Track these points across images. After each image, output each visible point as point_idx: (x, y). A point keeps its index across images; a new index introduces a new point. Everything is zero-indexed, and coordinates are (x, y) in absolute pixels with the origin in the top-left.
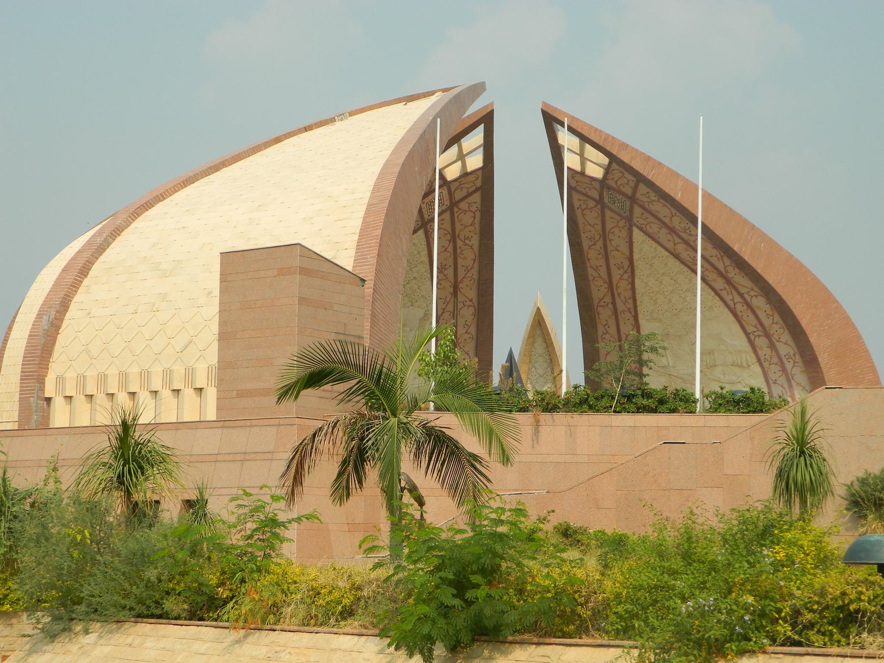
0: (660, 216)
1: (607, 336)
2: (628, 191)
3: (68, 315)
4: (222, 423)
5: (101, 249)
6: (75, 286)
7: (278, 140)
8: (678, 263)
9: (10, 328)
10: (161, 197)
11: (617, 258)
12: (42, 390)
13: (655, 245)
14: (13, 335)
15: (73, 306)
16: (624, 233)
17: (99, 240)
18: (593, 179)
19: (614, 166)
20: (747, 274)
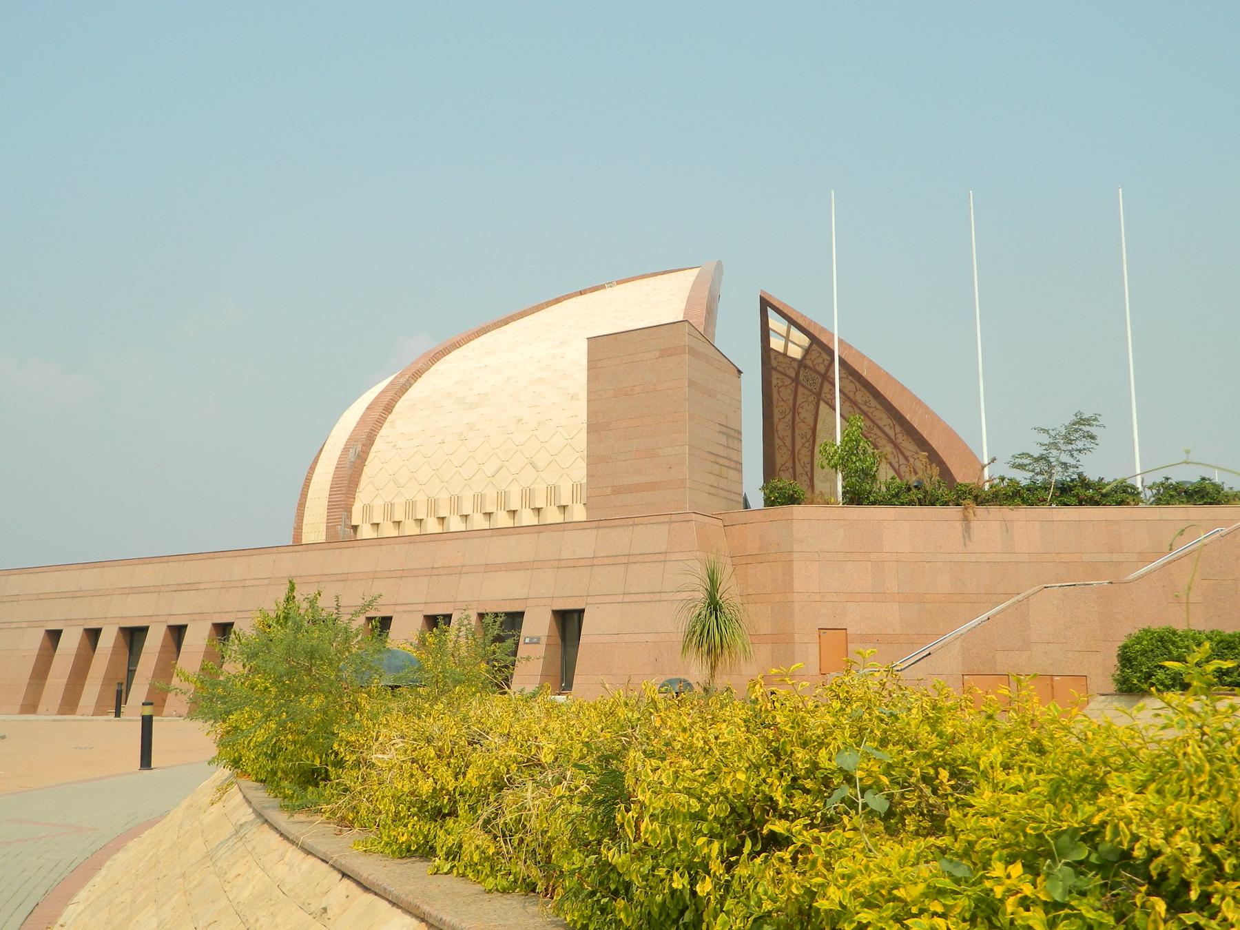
3: (373, 449)
4: (594, 523)
5: (404, 389)
6: (380, 422)
7: (558, 301)
9: (312, 469)
10: (457, 345)
11: (803, 428)
12: (349, 518)
14: (318, 470)
15: (378, 441)
16: (812, 407)
17: (402, 380)
18: (794, 359)
19: (815, 346)
20: (914, 440)
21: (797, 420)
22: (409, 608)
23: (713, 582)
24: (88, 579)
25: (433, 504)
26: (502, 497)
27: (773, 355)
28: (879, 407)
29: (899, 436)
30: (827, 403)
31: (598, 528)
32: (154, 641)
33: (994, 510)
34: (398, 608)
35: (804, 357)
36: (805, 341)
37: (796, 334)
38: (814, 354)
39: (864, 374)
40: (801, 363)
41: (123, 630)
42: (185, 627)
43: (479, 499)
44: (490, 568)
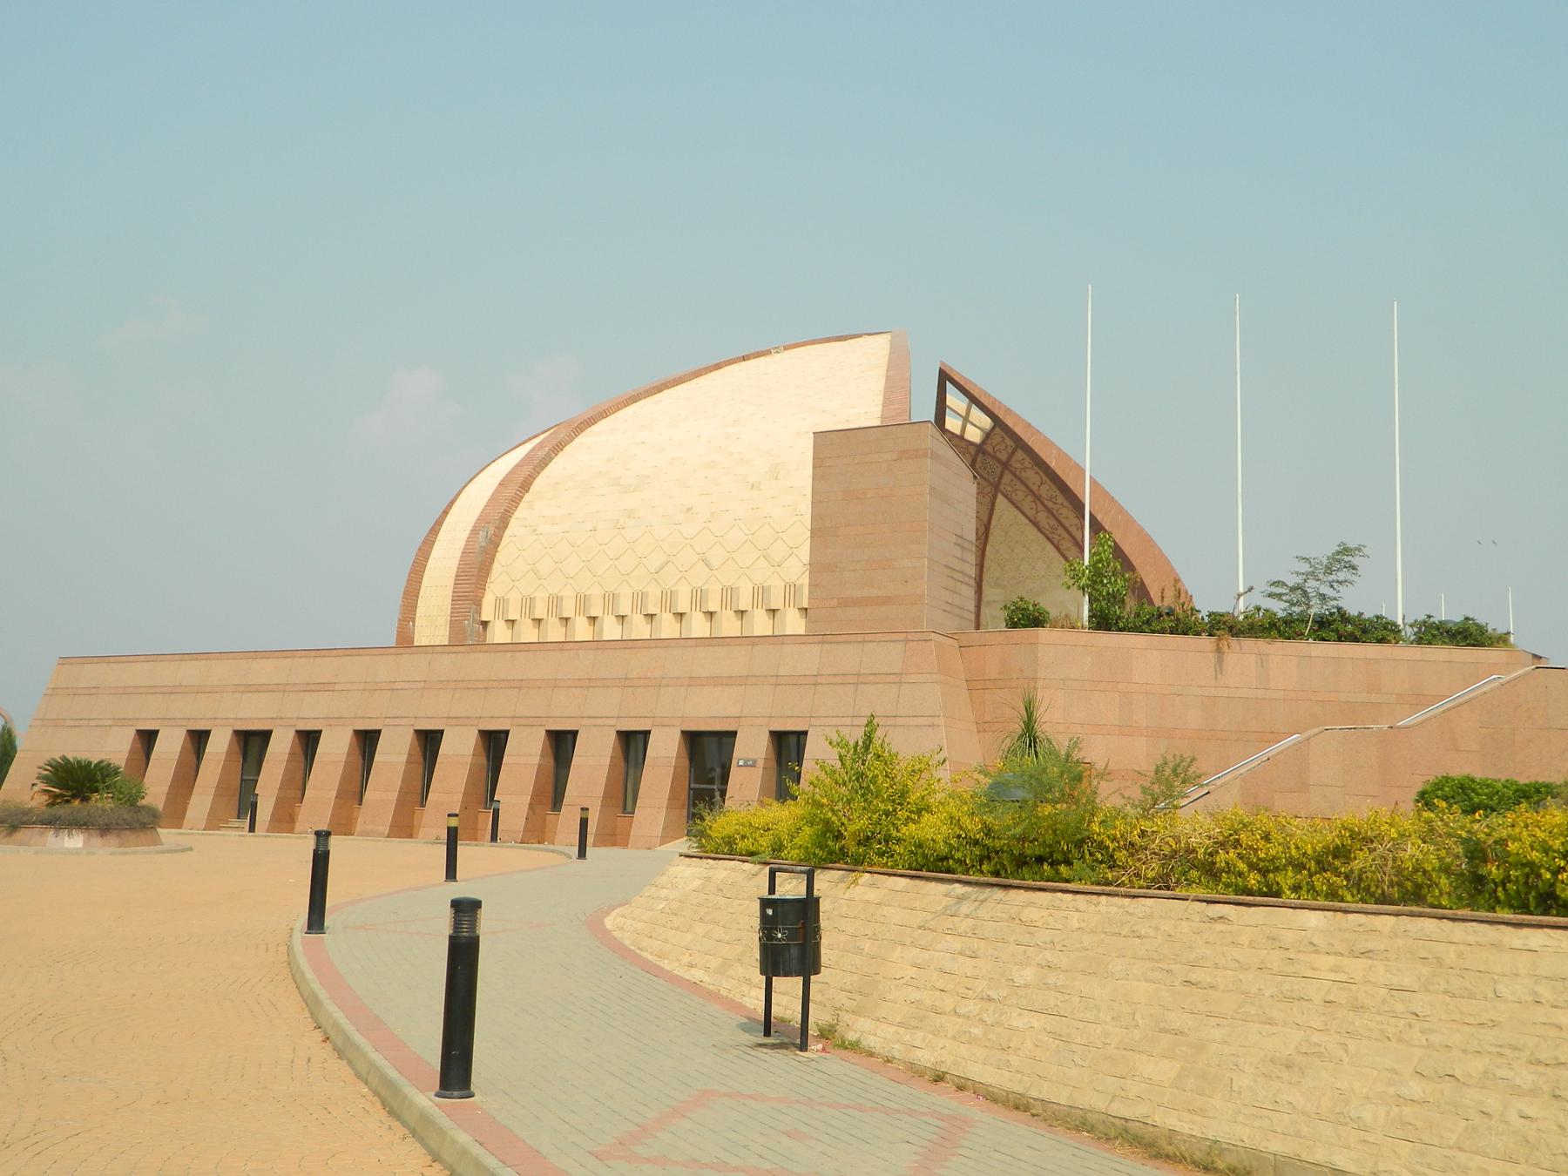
0: (1029, 483)
2: (1003, 456)
3: (508, 532)
5: (544, 463)
6: (516, 501)
7: (718, 367)
8: (1035, 531)
10: (604, 414)
13: (1016, 512)
14: (437, 552)
15: (513, 523)
17: (541, 454)
19: (998, 430)
22: (598, 722)
23: (1030, 714)
24: (190, 673)
26: (668, 598)
30: (1006, 496)
32: (280, 748)
33: (1249, 643)
34: (585, 721)
35: (984, 442)
36: (986, 422)
37: (977, 415)
38: (996, 439)
39: (1053, 465)
41: (237, 733)
42: (156, 732)
43: (640, 598)
44: (693, 682)
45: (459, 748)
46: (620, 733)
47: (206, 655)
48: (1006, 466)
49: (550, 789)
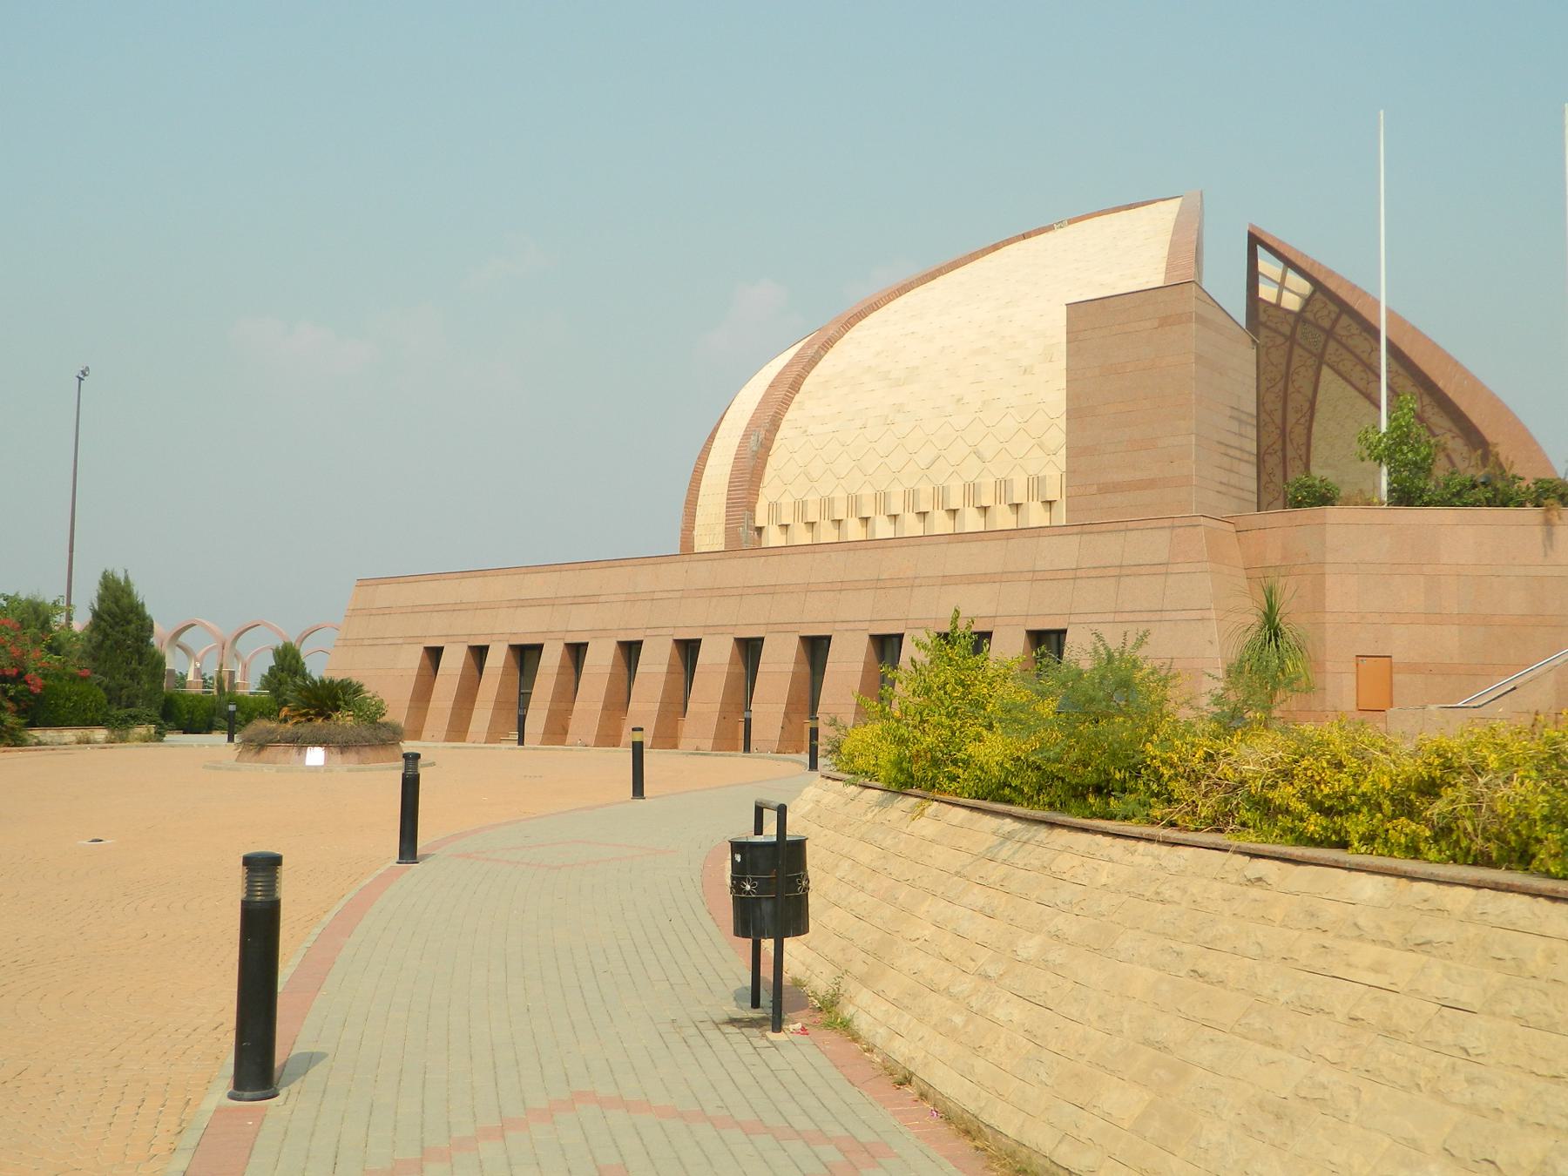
0: (1358, 351)
1: (1271, 486)
2: (1326, 324)
3: (779, 435)
4: (1078, 527)
5: (813, 362)
6: (786, 403)
7: (995, 247)
10: (874, 307)
13: (1345, 384)
17: (810, 352)
18: (1289, 312)
19: (1318, 295)
21: (1291, 389)
22: (851, 626)
24: (469, 590)
25: (854, 502)
26: (940, 494)
27: (1262, 307)
28: (1401, 371)
29: (1428, 409)
30: (1331, 367)
31: (1082, 533)
32: (551, 660)
34: (838, 626)
35: (1303, 310)
36: (1305, 287)
37: (1293, 279)
40: (1299, 317)
41: (512, 647)
43: (911, 495)
45: (716, 656)
46: (873, 637)
47: (483, 572)
48: (1330, 333)
49: (807, 697)
